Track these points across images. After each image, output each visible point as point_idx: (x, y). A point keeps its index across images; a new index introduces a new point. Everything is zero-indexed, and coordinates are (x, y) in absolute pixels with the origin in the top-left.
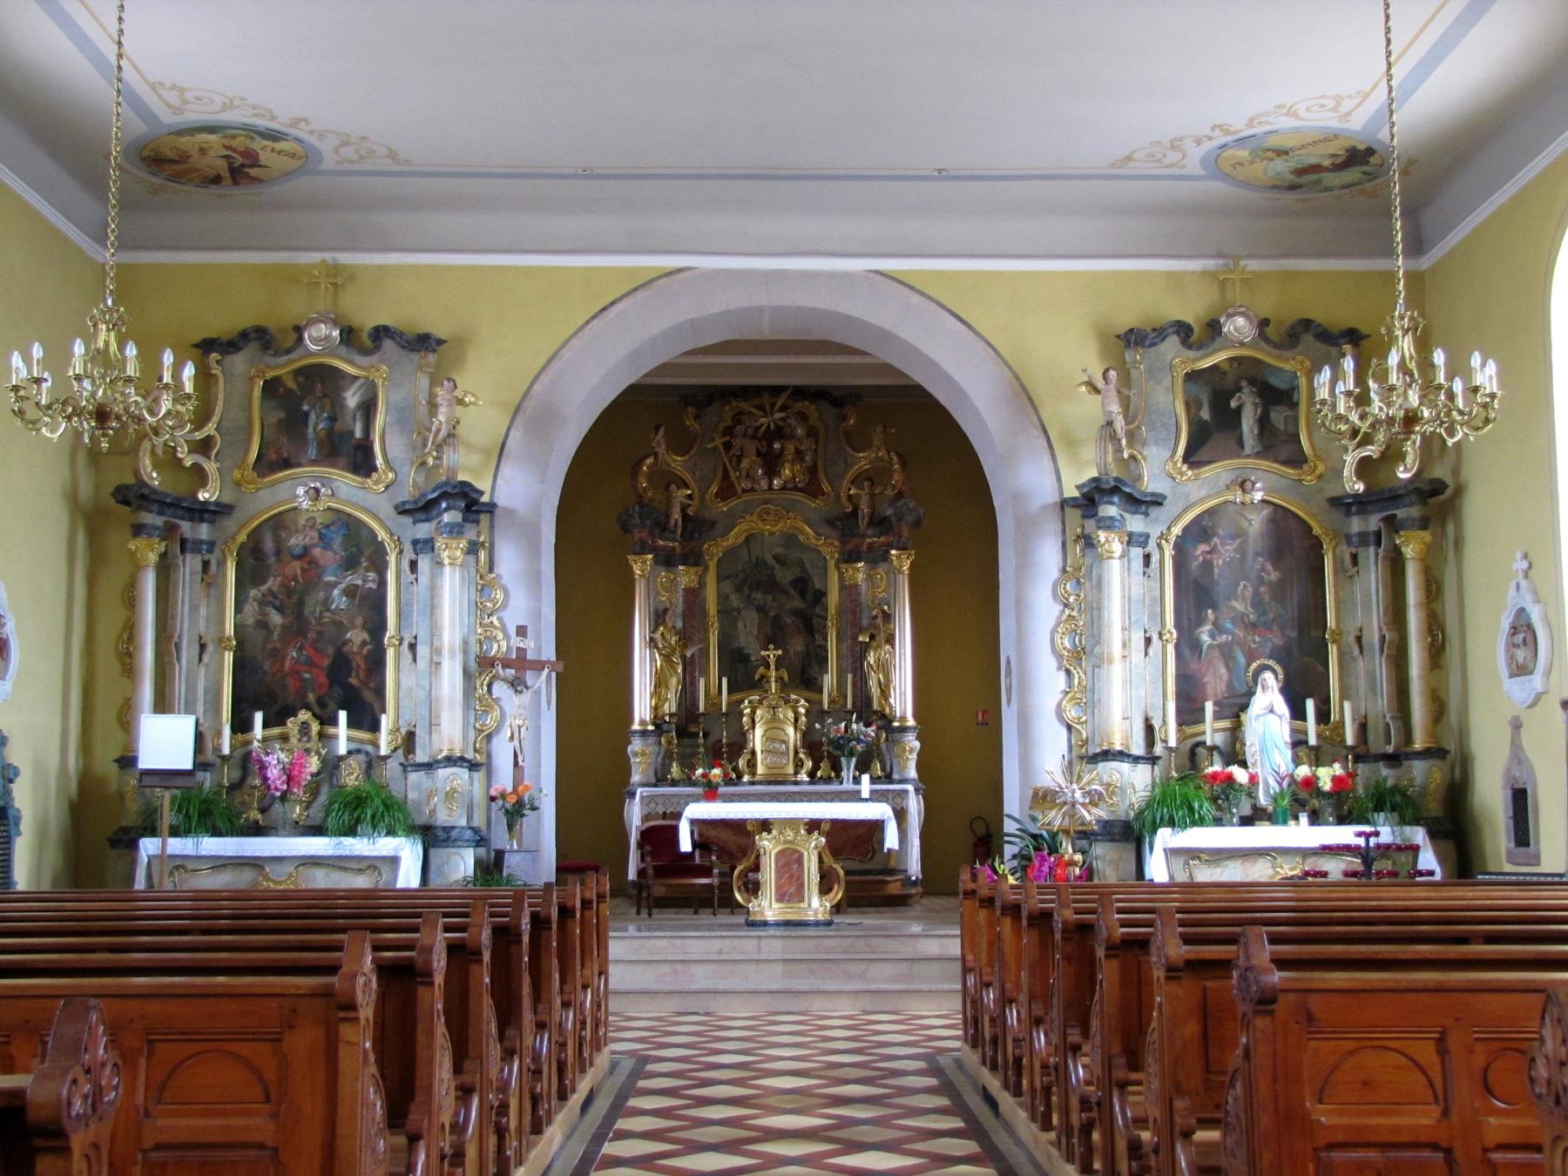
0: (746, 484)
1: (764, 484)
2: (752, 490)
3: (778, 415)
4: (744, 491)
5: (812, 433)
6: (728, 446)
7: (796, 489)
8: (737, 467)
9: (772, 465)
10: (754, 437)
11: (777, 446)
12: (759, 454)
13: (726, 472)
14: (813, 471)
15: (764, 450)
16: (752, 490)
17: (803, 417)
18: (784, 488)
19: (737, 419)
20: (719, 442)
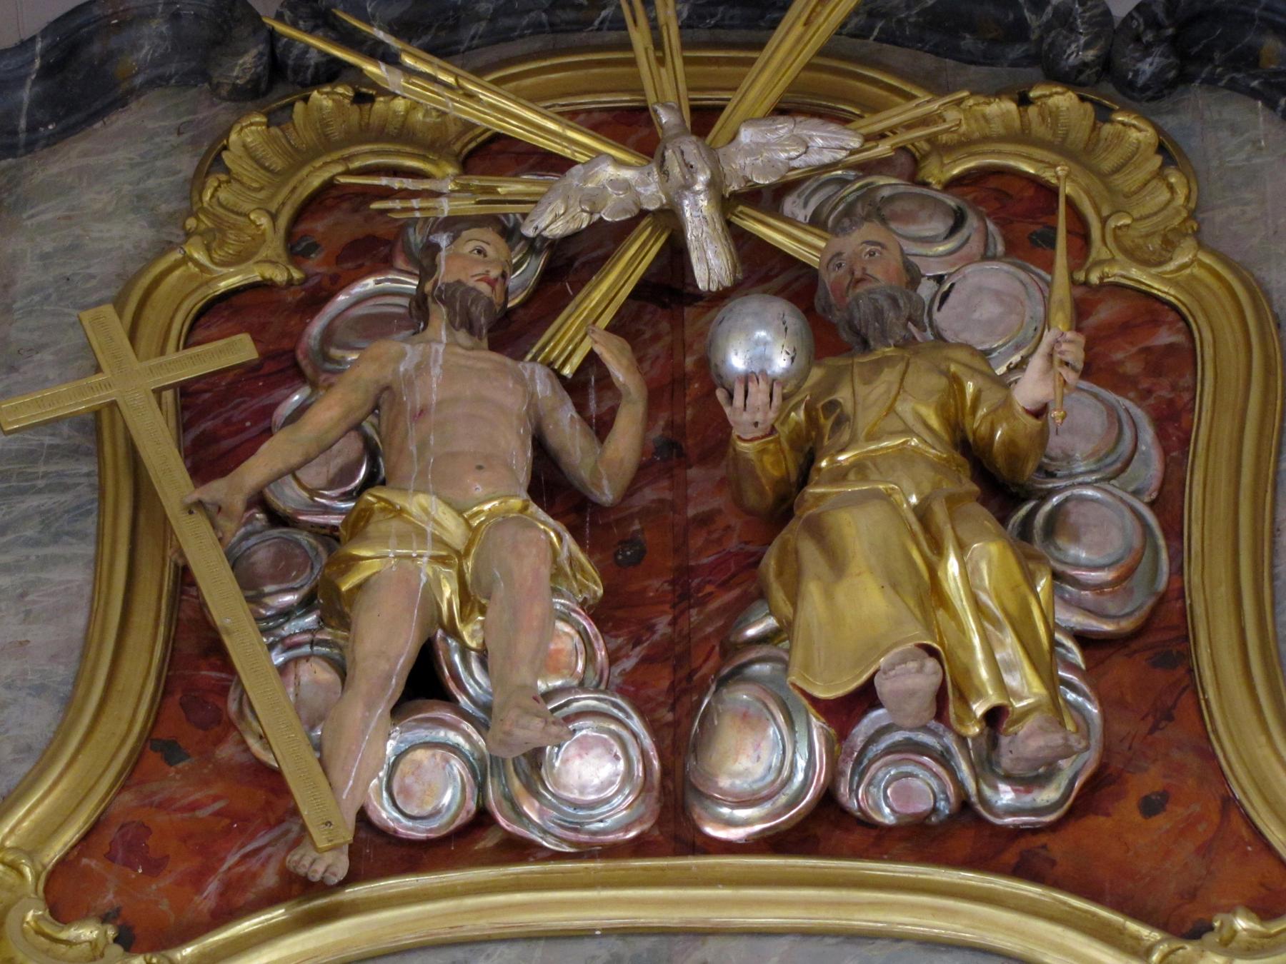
0: (430, 781)
1: (596, 772)
2: (476, 838)
3: (767, 147)
4: (379, 851)
5: (1136, 349)
6: (217, 425)
7: (956, 837)
8: (313, 565)
9: (682, 565)
10: (510, 331)
11: (758, 348)
12: (551, 484)
13: (196, 675)
14: (1144, 658)
15: (608, 462)
16: (476, 838)
17: (1021, 216)
18: (822, 828)
19: (346, 230)
20: (140, 387)
